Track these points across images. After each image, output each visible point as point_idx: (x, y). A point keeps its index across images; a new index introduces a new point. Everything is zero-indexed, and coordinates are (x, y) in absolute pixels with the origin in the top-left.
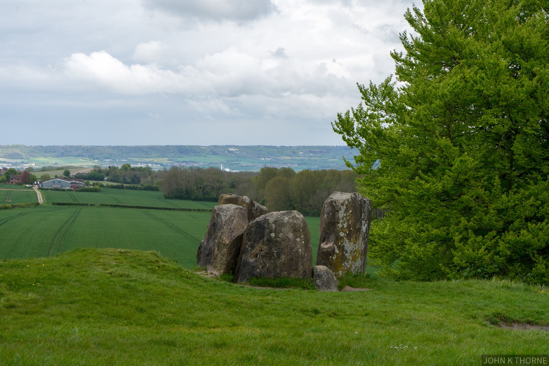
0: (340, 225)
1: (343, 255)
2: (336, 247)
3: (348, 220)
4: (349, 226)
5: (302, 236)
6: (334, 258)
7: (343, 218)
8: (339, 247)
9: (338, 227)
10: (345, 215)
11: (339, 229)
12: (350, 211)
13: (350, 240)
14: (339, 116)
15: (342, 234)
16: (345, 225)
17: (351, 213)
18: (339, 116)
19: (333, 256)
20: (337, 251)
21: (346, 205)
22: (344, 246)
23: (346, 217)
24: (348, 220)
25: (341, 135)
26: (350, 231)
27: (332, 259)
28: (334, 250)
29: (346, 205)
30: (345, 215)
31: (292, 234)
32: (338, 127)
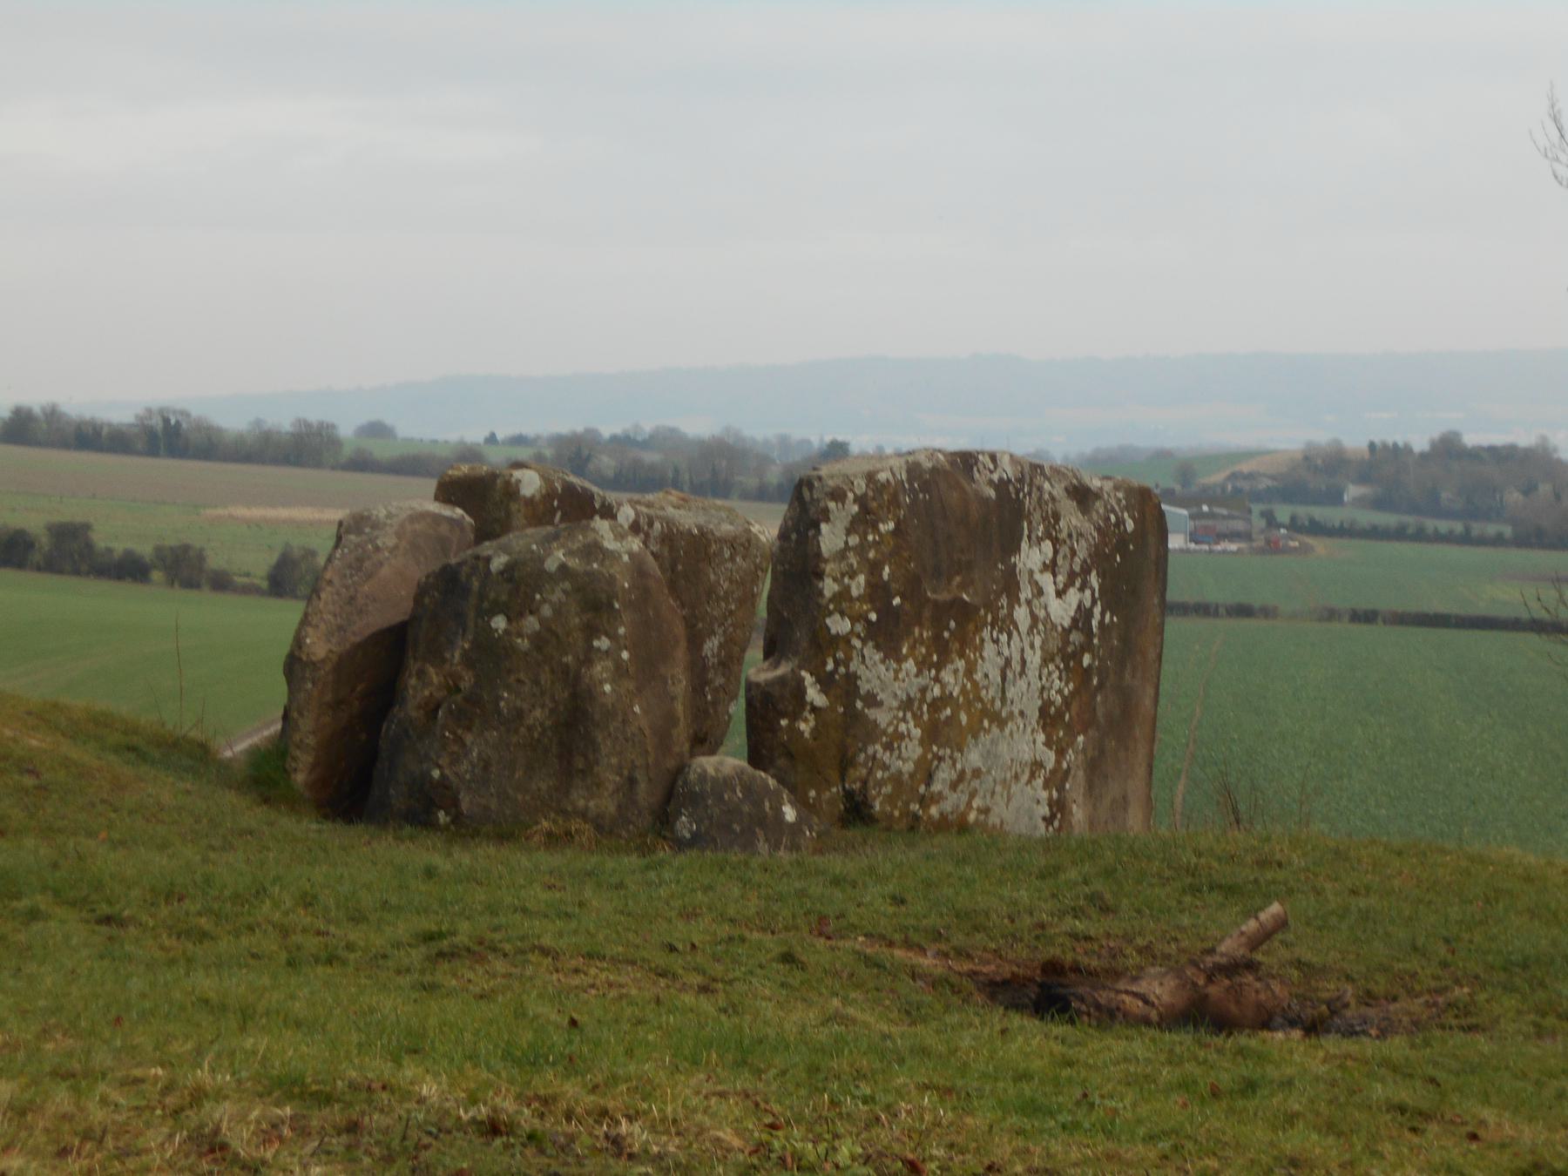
0: (829, 587)
1: (853, 719)
2: (809, 679)
4: (878, 592)
5: (622, 630)
6: (803, 726)
7: (842, 555)
8: (826, 683)
9: (821, 593)
10: (854, 540)
11: (824, 602)
12: (887, 526)
13: (891, 652)
15: (839, 625)
16: (858, 585)
19: (795, 716)
20: (814, 695)
21: (861, 500)
22: (852, 678)
23: (861, 550)
24: (874, 568)
26: (886, 611)
27: (792, 729)
28: (800, 691)
29: (861, 500)
30: (854, 540)
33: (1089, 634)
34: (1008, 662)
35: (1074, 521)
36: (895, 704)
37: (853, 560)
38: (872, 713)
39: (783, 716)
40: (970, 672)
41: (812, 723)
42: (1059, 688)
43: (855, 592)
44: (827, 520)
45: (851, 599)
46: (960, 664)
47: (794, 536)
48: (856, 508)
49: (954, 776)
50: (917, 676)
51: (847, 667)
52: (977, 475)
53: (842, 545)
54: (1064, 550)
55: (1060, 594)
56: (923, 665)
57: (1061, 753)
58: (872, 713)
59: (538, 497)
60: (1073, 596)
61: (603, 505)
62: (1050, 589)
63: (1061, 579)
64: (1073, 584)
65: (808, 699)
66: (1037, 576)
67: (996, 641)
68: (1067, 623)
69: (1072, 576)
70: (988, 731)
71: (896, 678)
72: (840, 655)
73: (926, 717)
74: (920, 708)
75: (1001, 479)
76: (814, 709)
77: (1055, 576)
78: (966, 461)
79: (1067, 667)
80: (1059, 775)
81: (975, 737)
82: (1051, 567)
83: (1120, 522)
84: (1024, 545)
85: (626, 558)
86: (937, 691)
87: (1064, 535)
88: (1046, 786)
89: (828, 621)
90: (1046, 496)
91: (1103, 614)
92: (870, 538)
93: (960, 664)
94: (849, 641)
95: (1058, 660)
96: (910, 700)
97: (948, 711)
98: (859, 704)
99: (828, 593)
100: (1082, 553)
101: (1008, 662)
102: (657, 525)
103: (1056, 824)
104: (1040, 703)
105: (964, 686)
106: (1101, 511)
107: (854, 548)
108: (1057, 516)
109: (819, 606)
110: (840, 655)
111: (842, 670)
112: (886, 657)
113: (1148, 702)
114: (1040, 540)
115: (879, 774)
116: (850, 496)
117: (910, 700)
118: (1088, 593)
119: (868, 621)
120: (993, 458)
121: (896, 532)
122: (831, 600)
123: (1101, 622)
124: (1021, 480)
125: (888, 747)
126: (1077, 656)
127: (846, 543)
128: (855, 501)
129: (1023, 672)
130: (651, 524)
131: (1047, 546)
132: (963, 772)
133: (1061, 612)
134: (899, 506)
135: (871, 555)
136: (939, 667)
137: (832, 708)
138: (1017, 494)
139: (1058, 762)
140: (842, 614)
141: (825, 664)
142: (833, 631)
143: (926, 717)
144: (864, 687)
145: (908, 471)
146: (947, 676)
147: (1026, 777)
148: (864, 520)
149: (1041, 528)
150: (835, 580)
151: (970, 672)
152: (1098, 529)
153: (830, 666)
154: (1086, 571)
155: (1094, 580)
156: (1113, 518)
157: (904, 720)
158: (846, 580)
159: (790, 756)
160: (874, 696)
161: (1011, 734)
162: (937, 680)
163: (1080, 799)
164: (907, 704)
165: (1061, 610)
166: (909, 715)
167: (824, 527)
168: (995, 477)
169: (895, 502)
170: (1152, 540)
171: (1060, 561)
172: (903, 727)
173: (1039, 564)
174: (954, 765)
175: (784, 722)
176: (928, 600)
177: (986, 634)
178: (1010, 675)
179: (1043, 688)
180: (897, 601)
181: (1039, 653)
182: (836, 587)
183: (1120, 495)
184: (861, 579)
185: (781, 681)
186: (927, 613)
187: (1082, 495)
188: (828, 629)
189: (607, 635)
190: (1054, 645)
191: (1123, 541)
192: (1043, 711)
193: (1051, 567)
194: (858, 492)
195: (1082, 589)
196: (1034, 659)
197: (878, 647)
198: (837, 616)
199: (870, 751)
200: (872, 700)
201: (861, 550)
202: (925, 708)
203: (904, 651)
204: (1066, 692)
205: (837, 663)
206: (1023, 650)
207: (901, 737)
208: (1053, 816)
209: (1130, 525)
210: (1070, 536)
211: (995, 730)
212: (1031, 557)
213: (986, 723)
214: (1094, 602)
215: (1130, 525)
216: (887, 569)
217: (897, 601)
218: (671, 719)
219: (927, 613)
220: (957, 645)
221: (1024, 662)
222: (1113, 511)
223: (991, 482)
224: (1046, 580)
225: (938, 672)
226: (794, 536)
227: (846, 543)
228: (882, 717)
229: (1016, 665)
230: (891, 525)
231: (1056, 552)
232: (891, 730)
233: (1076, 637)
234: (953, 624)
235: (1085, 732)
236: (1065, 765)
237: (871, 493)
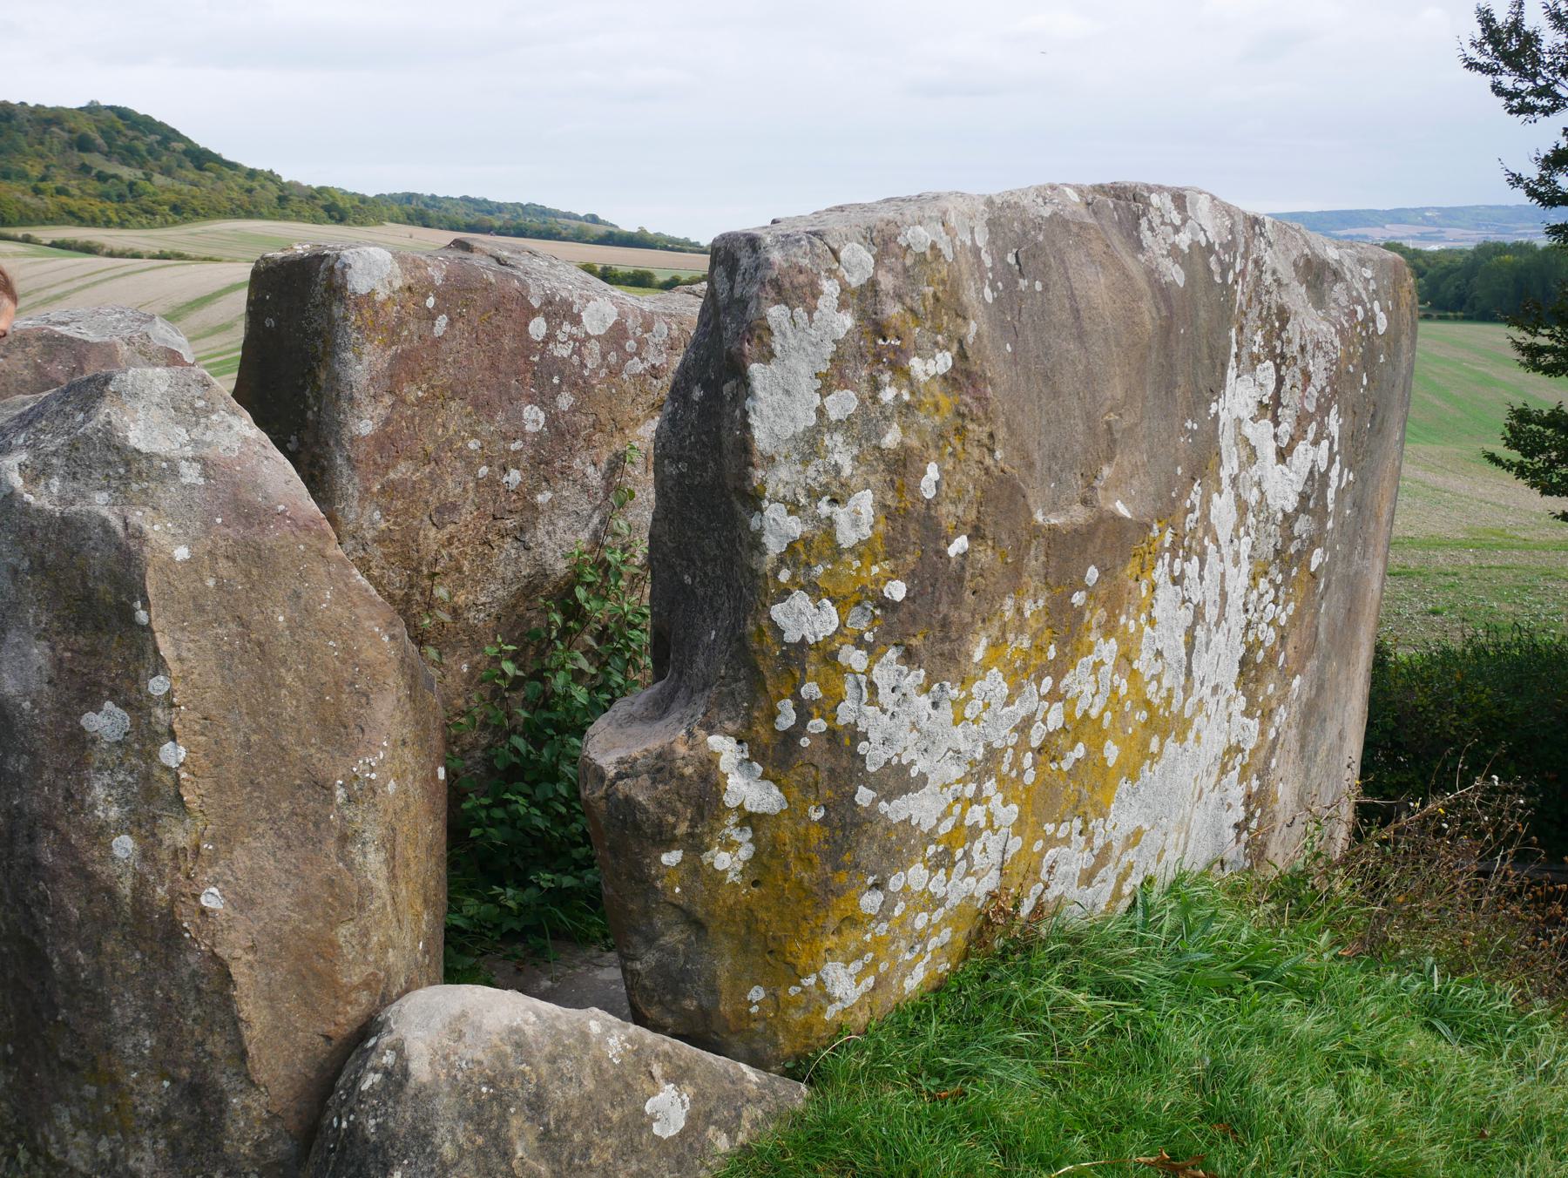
0: (779, 527)
1: (847, 825)
3: (901, 466)
4: (910, 529)
6: (722, 860)
7: (810, 446)
8: (775, 755)
9: (757, 545)
10: (842, 404)
12: (931, 366)
14: (1486, 19)
15: (803, 618)
16: (856, 520)
17: (962, 377)
18: (1486, 19)
20: (746, 789)
21: (864, 299)
22: (844, 741)
23: (862, 428)
25: (1488, 79)
27: (695, 869)
28: (705, 793)
29: (864, 299)
30: (842, 404)
31: (39, 653)
32: (1483, 52)
33: (1321, 514)
34: (1199, 614)
36: (956, 772)
37: (842, 454)
38: (896, 810)
39: (669, 845)
40: (1126, 657)
41: (745, 852)
43: (847, 536)
44: (768, 356)
45: (837, 552)
46: (1108, 650)
47: (697, 394)
48: (846, 321)
49: (1085, 860)
50: (1008, 702)
51: (830, 715)
52: (1147, 237)
53: (812, 420)
54: (1292, 375)
55: (1283, 455)
56: (1017, 677)
58: (896, 810)
59: (382, 296)
61: (549, 302)
62: (1268, 450)
63: (1286, 428)
65: (730, 801)
66: (1248, 429)
67: (1177, 581)
68: (1291, 504)
69: (1302, 419)
70: (1154, 758)
71: (959, 719)
72: (810, 690)
73: (1029, 778)
74: (1016, 763)
75: (1194, 245)
76: (749, 819)
77: (1277, 424)
78: (1127, 204)
80: (1262, 754)
81: (1133, 777)
82: (1270, 409)
83: (1371, 318)
84: (1231, 374)
85: (191, 474)
86: (1056, 718)
87: (1295, 348)
88: (1243, 778)
89: (777, 612)
90: (1268, 279)
91: (1340, 476)
92: (888, 395)
93: (1108, 650)
94: (830, 657)
95: (1273, 571)
96: (992, 754)
97: (1080, 751)
98: (864, 796)
99: (774, 546)
101: (1199, 614)
102: (660, 327)
104: (1242, 651)
105: (1114, 690)
106: (1343, 300)
107: (845, 425)
108: (1283, 315)
109: (754, 573)
110: (810, 690)
111: (817, 725)
112: (931, 679)
114: (1255, 360)
115: (921, 921)
116: (830, 288)
117: (992, 754)
118: (1325, 444)
119: (886, 605)
120: (1179, 199)
121: (951, 380)
122: (781, 560)
124: (1229, 246)
125: (944, 862)
126: (1302, 557)
127: (821, 412)
128: (843, 305)
129: (1222, 616)
130: (648, 327)
132: (1108, 847)
134: (961, 314)
135: (892, 438)
136: (1058, 670)
137: (794, 812)
138: (1225, 268)
139: (1263, 733)
140: (814, 590)
141: (773, 715)
142: (792, 636)
143: (1029, 778)
144: (875, 755)
145: (992, 224)
146: (1079, 681)
148: (876, 346)
149: (1258, 338)
150: (794, 508)
151: (1126, 657)
152: (1341, 332)
153: (787, 718)
154: (1323, 410)
155: (1334, 424)
157: (977, 799)
158: (824, 508)
159: (698, 926)
160: (903, 769)
162: (1054, 696)
164: (986, 766)
165: (1282, 487)
166: (990, 786)
167: (755, 369)
168: (1184, 240)
169: (950, 305)
170: (1405, 341)
172: (977, 814)
173: (1253, 408)
174: (1089, 841)
175: (671, 858)
176: (1036, 531)
177: (1160, 573)
178: (1200, 633)
180: (959, 545)
181: (1246, 567)
182: (795, 527)
183: (1368, 273)
184: (865, 502)
185: (661, 767)
186: (1035, 561)
187: (1317, 274)
188: (779, 632)
189: (126, 705)
190: (1267, 549)
194: (855, 281)
195: (1316, 443)
196: (1238, 581)
197: (909, 657)
198: (800, 600)
199: (895, 883)
200: (899, 781)
201: (862, 428)
202: (1028, 759)
203: (978, 654)
205: (804, 711)
206: (1223, 575)
207: (975, 832)
208: (1250, 816)
209: (1382, 325)
210: (1303, 349)
211: (1171, 746)
212: (1239, 397)
213: (1154, 745)
214: (1331, 461)
215: (1382, 325)
216: (932, 472)
217: (959, 545)
218: (345, 899)
219: (1035, 561)
220: (1101, 614)
221: (1224, 595)
223: (1174, 252)
224: (1262, 434)
225: (1058, 676)
226: (697, 394)
227: (821, 412)
228: (920, 809)
229: (1211, 613)
230: (943, 362)
231: (1280, 381)
232: (947, 825)
233: (1302, 525)
234: (1092, 574)
236: (1272, 734)
237: (887, 282)
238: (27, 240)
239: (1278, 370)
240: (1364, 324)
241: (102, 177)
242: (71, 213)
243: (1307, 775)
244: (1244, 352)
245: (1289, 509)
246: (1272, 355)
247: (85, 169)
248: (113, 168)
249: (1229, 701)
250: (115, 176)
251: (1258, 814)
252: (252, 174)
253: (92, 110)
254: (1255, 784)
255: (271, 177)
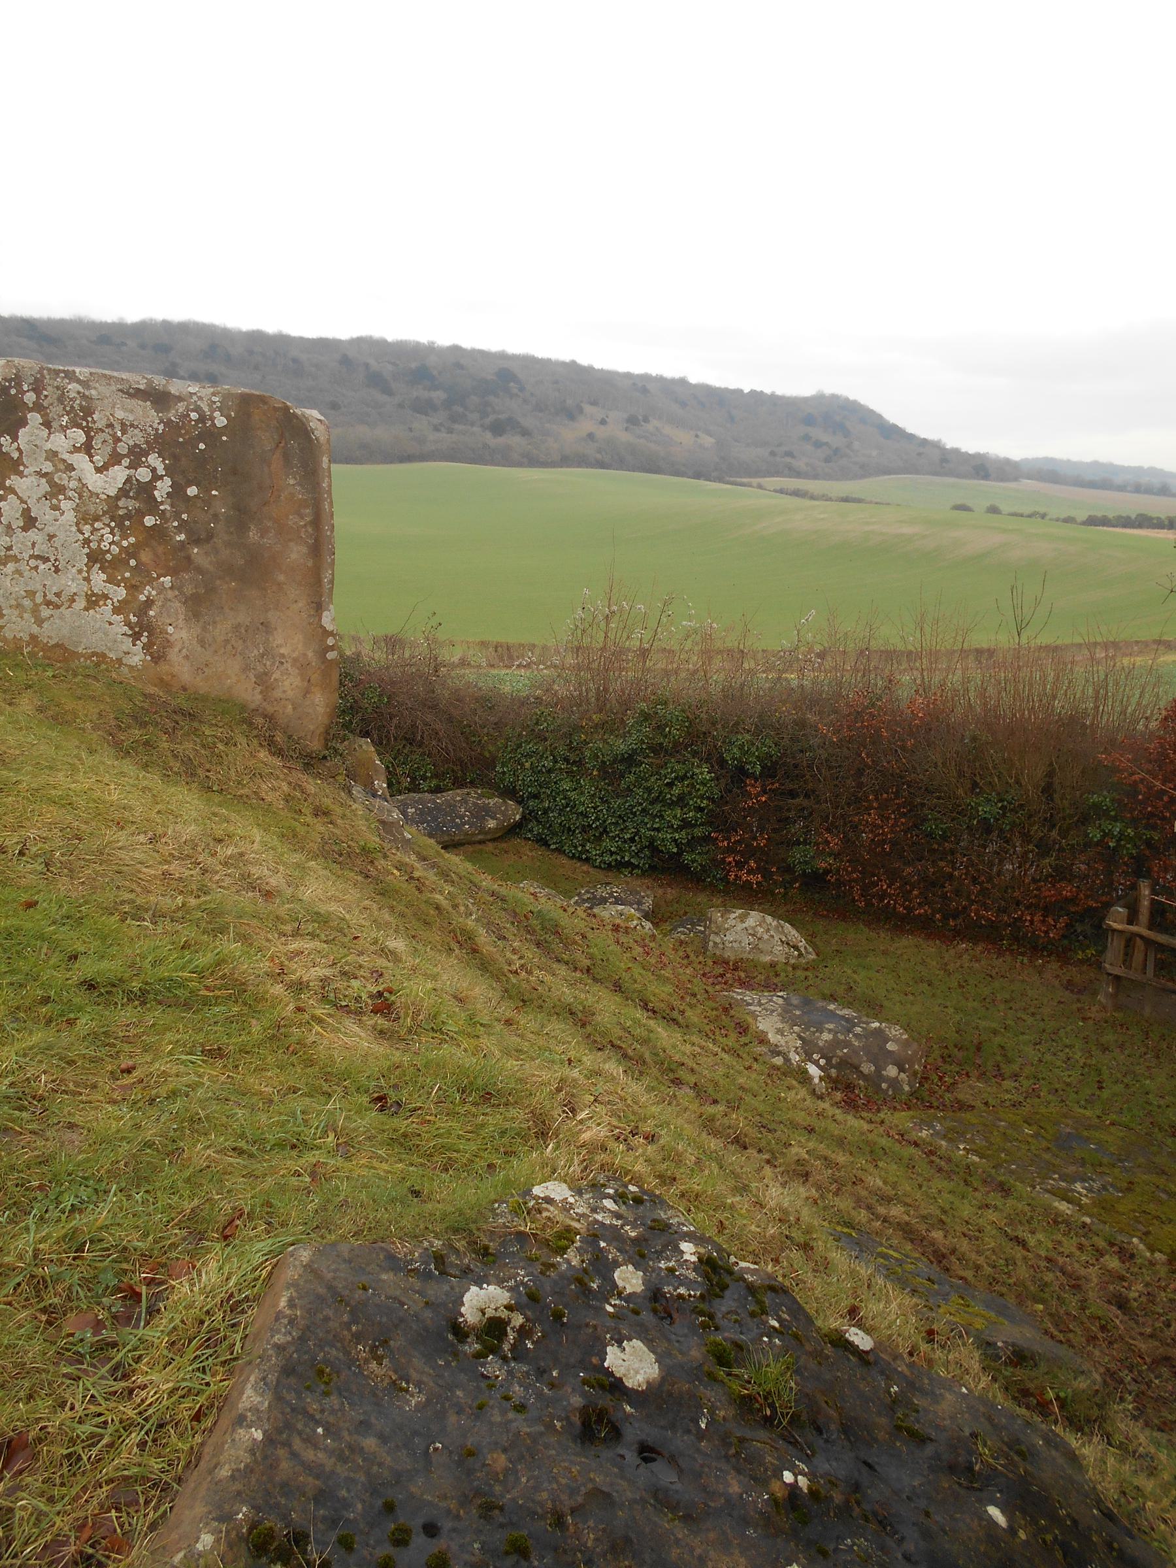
35: (120, 414)
42: (108, 539)
57: (133, 588)
60: (119, 474)
63: (99, 460)
64: (119, 463)
68: (112, 492)
77: (91, 456)
79: (120, 525)
95: (106, 520)
100: (135, 438)
103: (144, 639)
104: (86, 550)
108: (88, 412)
113: (296, 553)
123: (177, 492)
131: (79, 436)
133: (100, 483)
147: (81, 603)
152: (168, 423)
155: (154, 460)
156: (194, 416)
161: (18, 572)
163: (181, 623)
171: (97, 443)
179: (87, 542)
191: (210, 435)
192: (95, 557)
193: (88, 448)
195: (133, 466)
204: (125, 543)
206: (28, 510)
209: (221, 421)
214: (156, 477)
222: (198, 409)
224: (81, 461)
231: (90, 439)
235: (173, 572)
236: (143, 598)
238: (760, 487)
239: (87, 434)
240: (202, 419)
241: (818, 444)
242: (790, 468)
243: (204, 629)
244: (55, 425)
245: (112, 494)
246: (79, 426)
247: (806, 438)
248: (825, 438)
249: (80, 571)
250: (826, 444)
251: (146, 634)
252: (925, 442)
253: (820, 398)
254: (133, 619)
255: (936, 445)
